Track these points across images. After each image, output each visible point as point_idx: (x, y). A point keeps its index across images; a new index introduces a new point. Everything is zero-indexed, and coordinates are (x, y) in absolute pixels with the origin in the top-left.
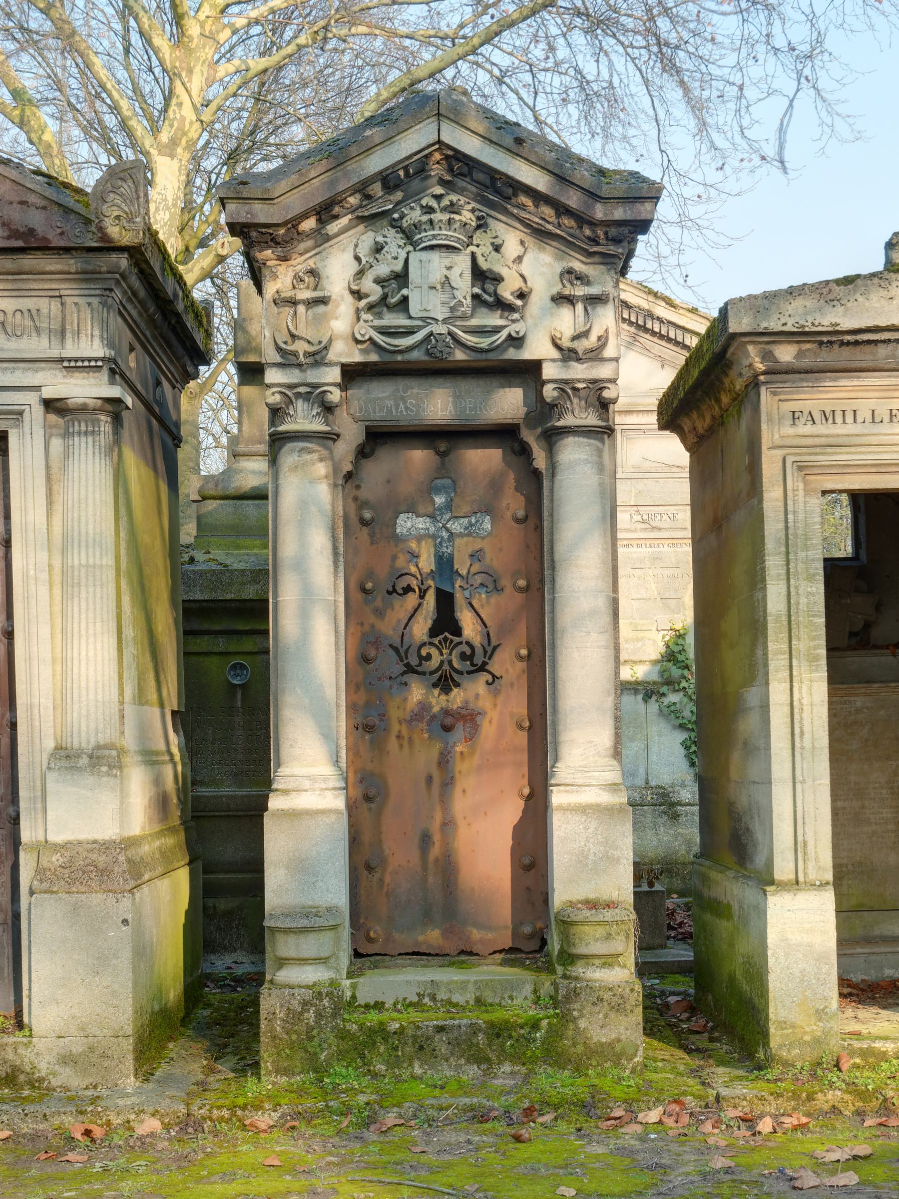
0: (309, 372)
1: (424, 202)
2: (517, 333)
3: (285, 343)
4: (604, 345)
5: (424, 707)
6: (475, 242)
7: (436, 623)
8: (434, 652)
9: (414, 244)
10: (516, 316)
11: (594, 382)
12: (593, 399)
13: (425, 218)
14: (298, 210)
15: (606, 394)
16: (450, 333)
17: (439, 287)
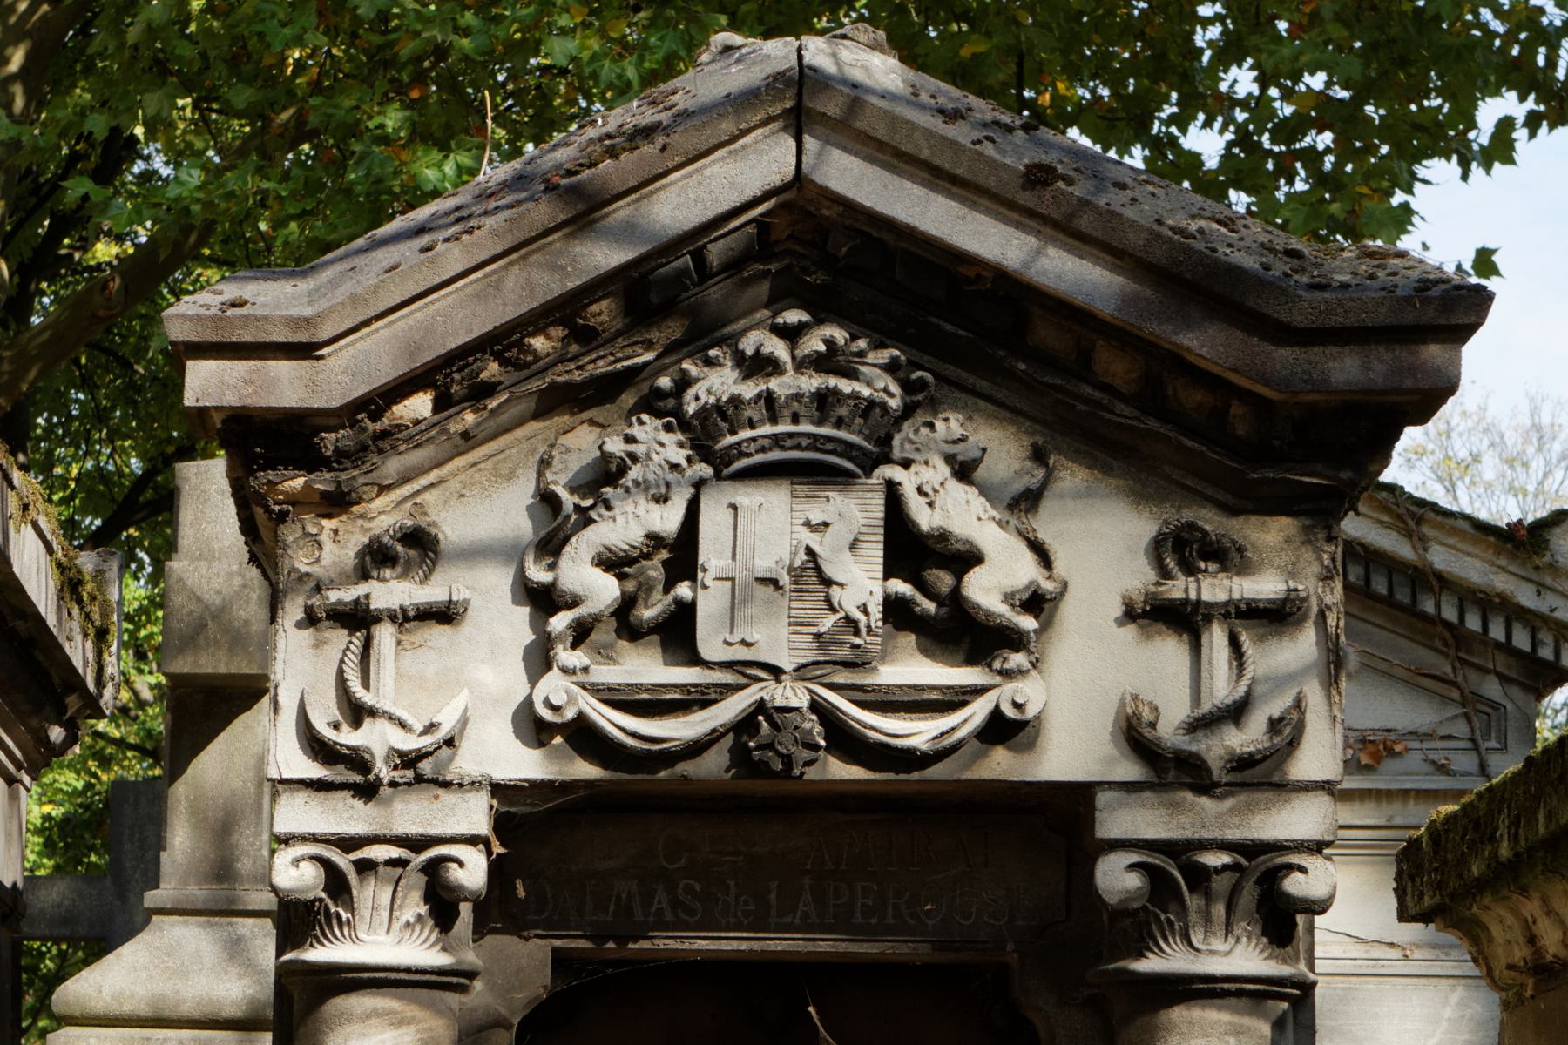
0: (398, 805)
1: (748, 345)
2: (1018, 706)
3: (336, 727)
4: (1293, 744)
6: (897, 453)
10: (1018, 659)
11: (1252, 849)
12: (1249, 895)
13: (749, 390)
14: (386, 371)
15: (1294, 885)
16: (816, 706)
17: (785, 580)
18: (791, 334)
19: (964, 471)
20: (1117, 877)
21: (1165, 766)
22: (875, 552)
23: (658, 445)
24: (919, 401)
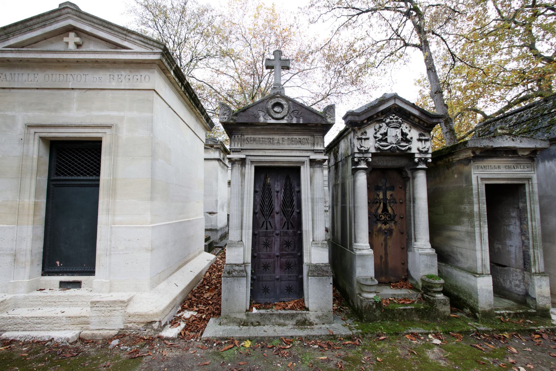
5: (381, 228)
9: (389, 126)
18: (394, 116)
20: (416, 160)
21: (421, 152)
23: (384, 124)
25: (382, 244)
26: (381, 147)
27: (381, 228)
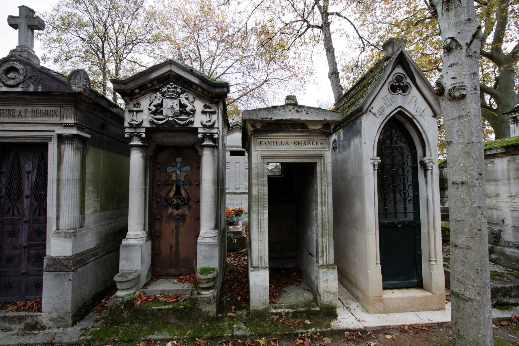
5: (172, 213)
7: (175, 193)
8: (175, 200)
9: (164, 97)
16: (174, 120)
18: (171, 85)
19: (187, 99)
22: (178, 105)
23: (159, 94)
24: (183, 92)
25: (173, 231)
26: (155, 121)
27: (172, 213)
